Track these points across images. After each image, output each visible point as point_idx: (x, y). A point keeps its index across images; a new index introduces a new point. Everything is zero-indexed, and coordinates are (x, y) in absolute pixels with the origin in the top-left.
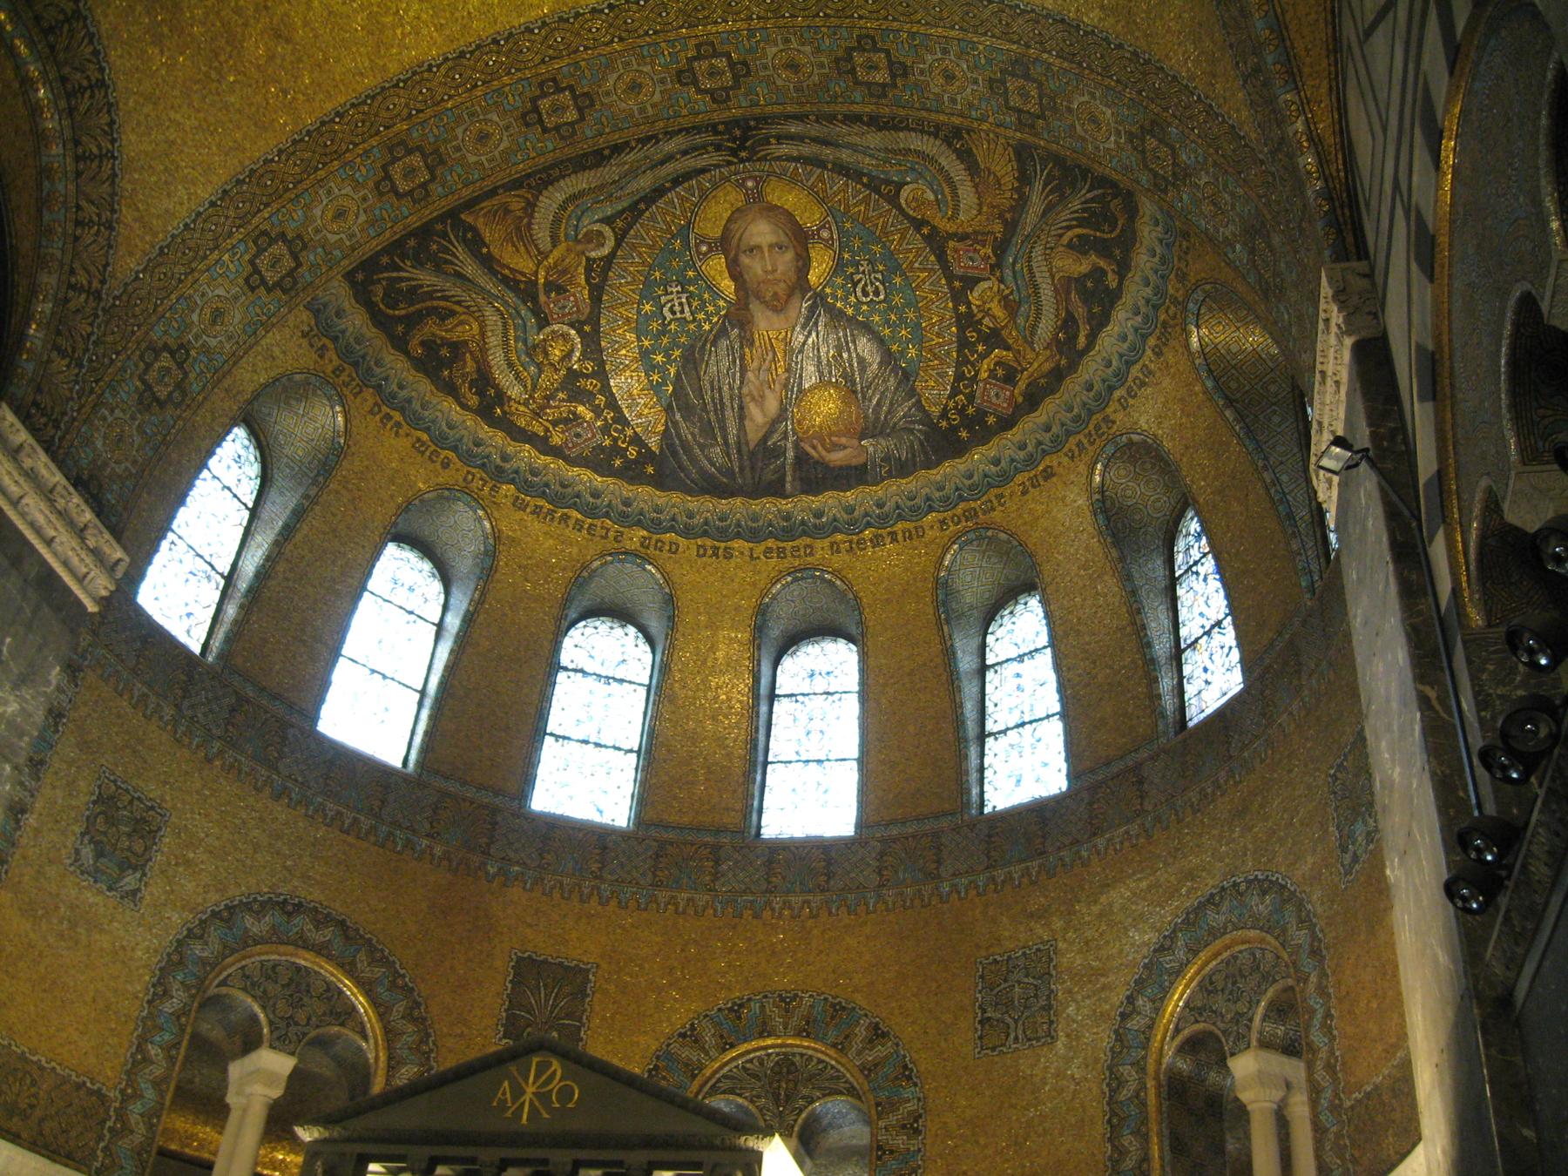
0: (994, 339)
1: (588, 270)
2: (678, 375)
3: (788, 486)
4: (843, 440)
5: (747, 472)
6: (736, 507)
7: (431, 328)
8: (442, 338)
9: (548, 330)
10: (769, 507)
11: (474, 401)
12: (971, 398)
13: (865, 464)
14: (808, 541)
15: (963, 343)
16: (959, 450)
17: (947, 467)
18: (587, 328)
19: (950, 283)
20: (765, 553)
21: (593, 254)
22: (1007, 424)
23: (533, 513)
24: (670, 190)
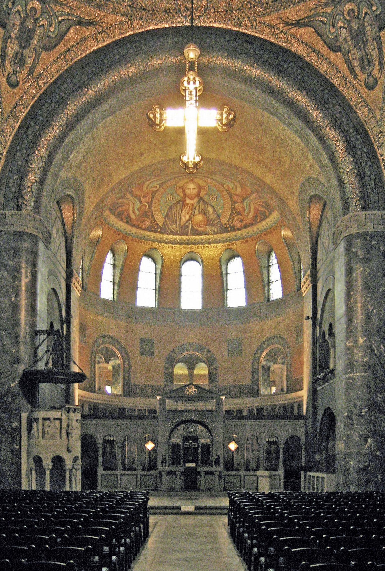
0: (239, 213)
2: (168, 211)
12: (232, 223)
14: (193, 246)
15: (232, 212)
16: (228, 232)
17: (225, 235)
19: (232, 202)
22: (239, 229)
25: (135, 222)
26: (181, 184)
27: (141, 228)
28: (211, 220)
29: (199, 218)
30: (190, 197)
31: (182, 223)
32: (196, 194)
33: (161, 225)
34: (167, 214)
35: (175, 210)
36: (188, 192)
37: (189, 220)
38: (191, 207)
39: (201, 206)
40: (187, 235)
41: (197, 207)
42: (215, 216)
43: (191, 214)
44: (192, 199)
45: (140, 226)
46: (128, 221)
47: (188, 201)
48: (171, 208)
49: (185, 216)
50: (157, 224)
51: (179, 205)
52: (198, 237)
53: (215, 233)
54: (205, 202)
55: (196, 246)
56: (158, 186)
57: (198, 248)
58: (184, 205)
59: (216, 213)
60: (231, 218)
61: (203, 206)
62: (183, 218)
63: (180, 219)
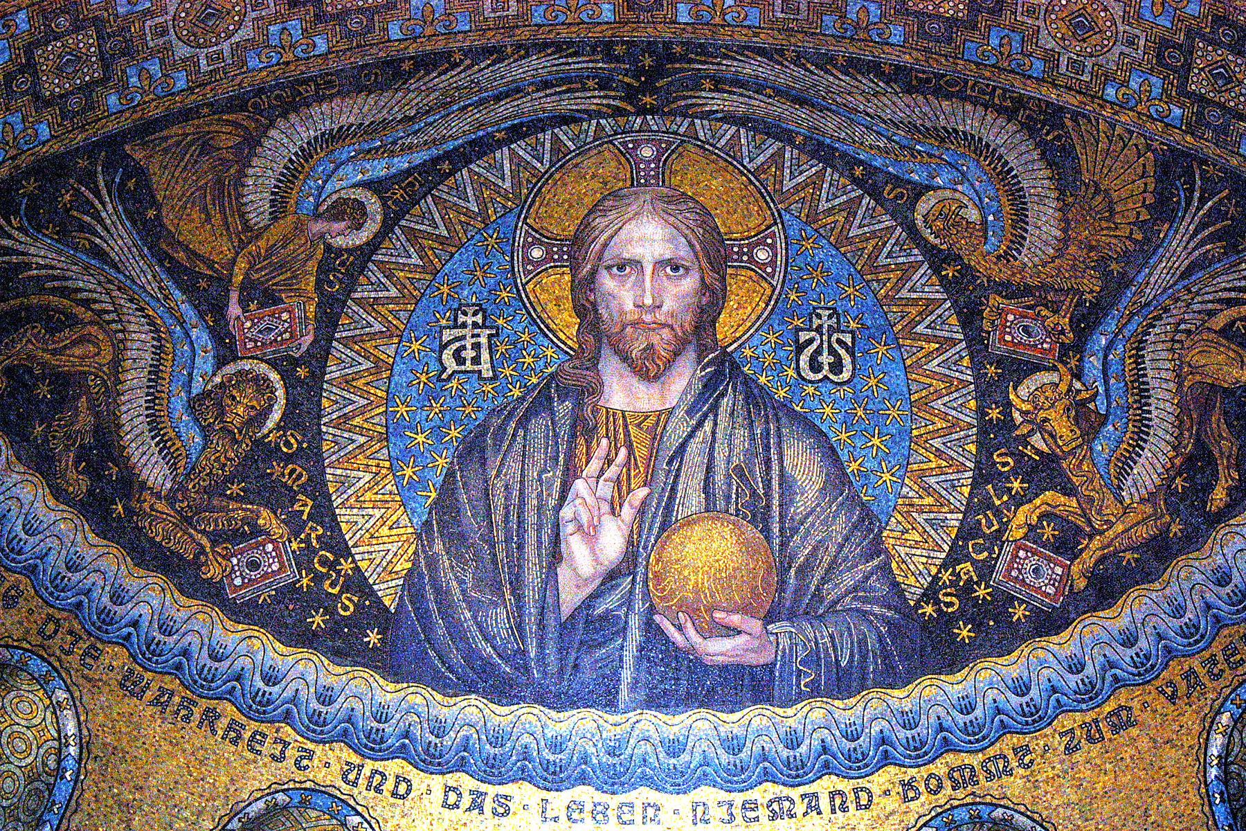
18: (301, 372)
21: (340, 241)
28: (803, 571)
29: (708, 552)
31: (570, 596)
33: (388, 593)
34: (446, 505)
35: (513, 467)
44: (648, 370)
47: (622, 393)
50: (358, 584)
51: (539, 425)
54: (755, 398)
61: (741, 434)
62: (576, 546)
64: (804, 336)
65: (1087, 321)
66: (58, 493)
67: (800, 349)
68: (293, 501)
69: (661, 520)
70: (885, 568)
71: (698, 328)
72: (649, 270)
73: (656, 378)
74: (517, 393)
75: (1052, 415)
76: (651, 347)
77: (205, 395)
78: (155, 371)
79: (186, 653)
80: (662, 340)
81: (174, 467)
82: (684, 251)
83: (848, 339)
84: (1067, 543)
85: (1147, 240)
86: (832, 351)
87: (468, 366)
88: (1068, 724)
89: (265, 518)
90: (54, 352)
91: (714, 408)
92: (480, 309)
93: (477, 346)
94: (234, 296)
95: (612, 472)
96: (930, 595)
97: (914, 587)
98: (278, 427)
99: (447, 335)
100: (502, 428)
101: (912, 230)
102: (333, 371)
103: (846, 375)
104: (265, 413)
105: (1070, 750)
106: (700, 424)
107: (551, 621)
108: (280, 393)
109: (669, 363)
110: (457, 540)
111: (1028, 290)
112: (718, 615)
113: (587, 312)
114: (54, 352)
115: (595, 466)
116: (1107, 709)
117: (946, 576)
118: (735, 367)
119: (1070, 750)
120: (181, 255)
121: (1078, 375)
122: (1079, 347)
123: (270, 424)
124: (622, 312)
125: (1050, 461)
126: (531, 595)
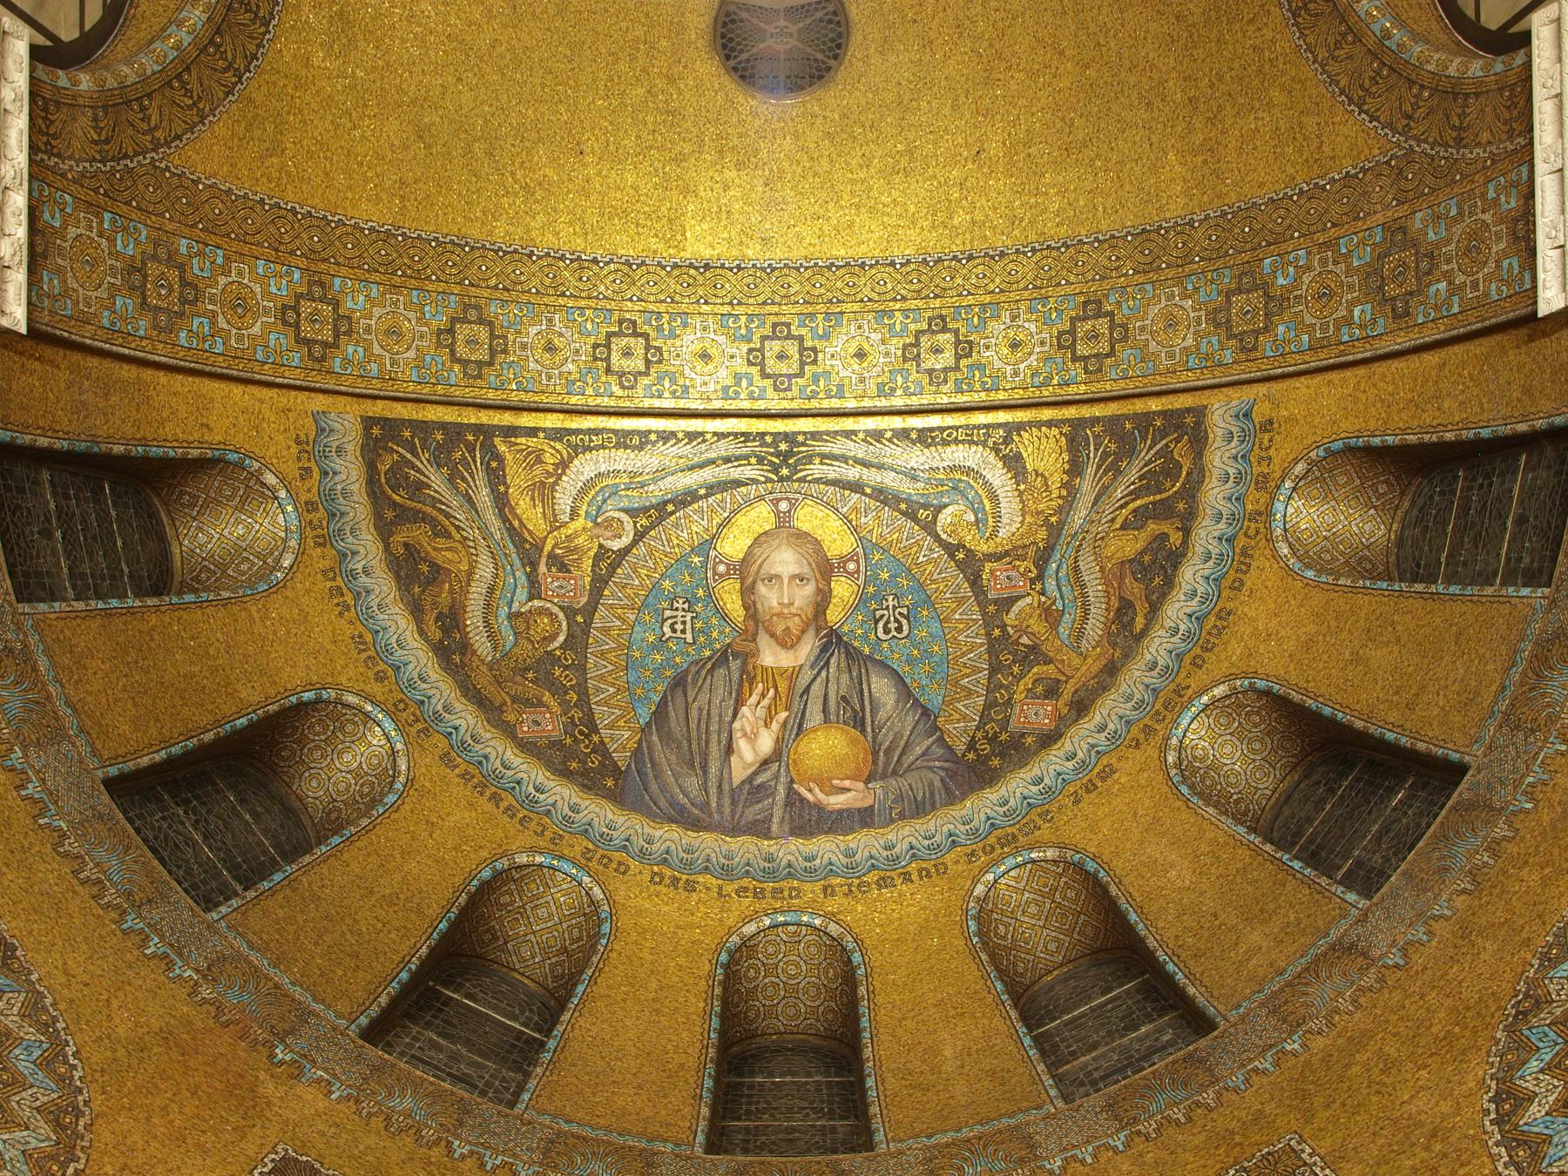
1: (598, 558)
3: (774, 828)
4: (847, 783)
5: (727, 810)
6: (709, 844)
7: (418, 534)
8: (427, 553)
9: (536, 603)
10: (744, 848)
11: (435, 633)
13: (872, 807)
18: (580, 619)
20: (737, 892)
23: (462, 776)
24: (701, 497)
25: (483, 681)
26: (733, 546)
27: (510, 732)
28: (889, 751)
29: (826, 746)
30: (779, 631)
31: (739, 773)
32: (810, 611)
33: (622, 758)
34: (660, 714)
35: (703, 698)
36: (770, 597)
37: (777, 755)
38: (783, 686)
39: (838, 680)
40: (767, 835)
41: (817, 688)
42: (910, 720)
43: (785, 724)
44: (787, 642)
45: (511, 717)
46: (451, 647)
47: (771, 656)
48: (679, 682)
49: (752, 738)
50: (601, 749)
52: (826, 848)
53: (920, 809)
54: (852, 654)
55: (818, 886)
56: (629, 526)
57: (828, 891)
58: (748, 676)
59: (916, 701)
60: (995, 703)
61: (845, 678)
62: (742, 745)
63: (729, 749)
64: (878, 613)
65: (1042, 560)
66: (421, 632)
67: (876, 622)
68: (566, 693)
69: (797, 728)
70: (941, 740)
71: (816, 617)
72: (786, 581)
73: (792, 646)
74: (708, 653)
75: (1031, 621)
76: (788, 628)
77: (519, 614)
78: (491, 590)
79: (486, 757)
80: (795, 624)
81: (495, 649)
82: (806, 569)
83: (904, 611)
84: (1052, 692)
85: (1069, 494)
86: (896, 620)
87: (679, 634)
88: (1072, 790)
89: (547, 697)
90: (435, 549)
91: (827, 663)
92: (687, 600)
93: (684, 623)
94: (544, 560)
95: (766, 702)
96: (971, 746)
97: (960, 747)
98: (561, 647)
99: (668, 613)
100: (698, 672)
101: (937, 538)
102: (597, 623)
103: (905, 633)
104: (554, 637)
105: (1077, 802)
106: (819, 673)
107: (726, 787)
108: (564, 624)
109: (799, 639)
110: (667, 738)
111: (1007, 554)
112: (835, 782)
113: (750, 608)
114: (435, 549)
115: (754, 699)
116: (1096, 771)
117: (979, 735)
118: (839, 638)
119: (1077, 802)
120: (516, 524)
121: (1042, 593)
122: (1040, 577)
123: (556, 644)
124: (771, 608)
125: (1033, 648)
126: (713, 770)
